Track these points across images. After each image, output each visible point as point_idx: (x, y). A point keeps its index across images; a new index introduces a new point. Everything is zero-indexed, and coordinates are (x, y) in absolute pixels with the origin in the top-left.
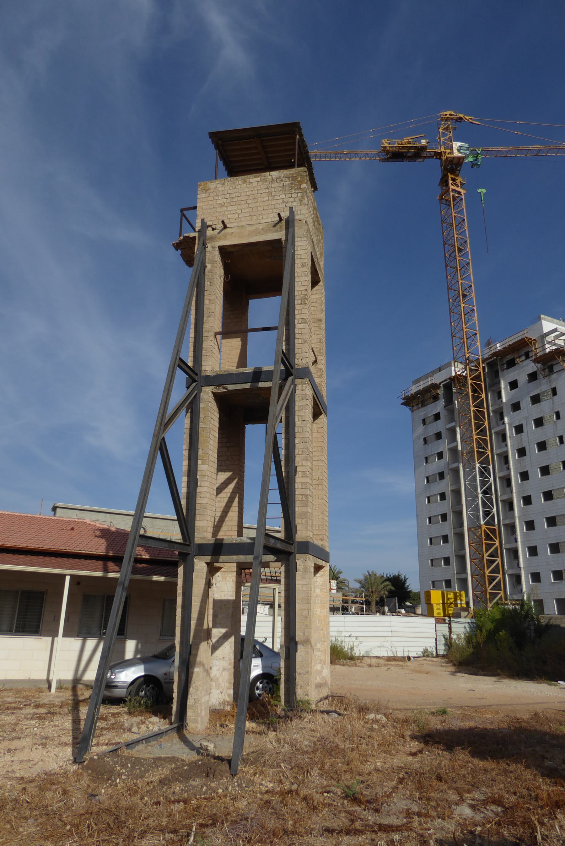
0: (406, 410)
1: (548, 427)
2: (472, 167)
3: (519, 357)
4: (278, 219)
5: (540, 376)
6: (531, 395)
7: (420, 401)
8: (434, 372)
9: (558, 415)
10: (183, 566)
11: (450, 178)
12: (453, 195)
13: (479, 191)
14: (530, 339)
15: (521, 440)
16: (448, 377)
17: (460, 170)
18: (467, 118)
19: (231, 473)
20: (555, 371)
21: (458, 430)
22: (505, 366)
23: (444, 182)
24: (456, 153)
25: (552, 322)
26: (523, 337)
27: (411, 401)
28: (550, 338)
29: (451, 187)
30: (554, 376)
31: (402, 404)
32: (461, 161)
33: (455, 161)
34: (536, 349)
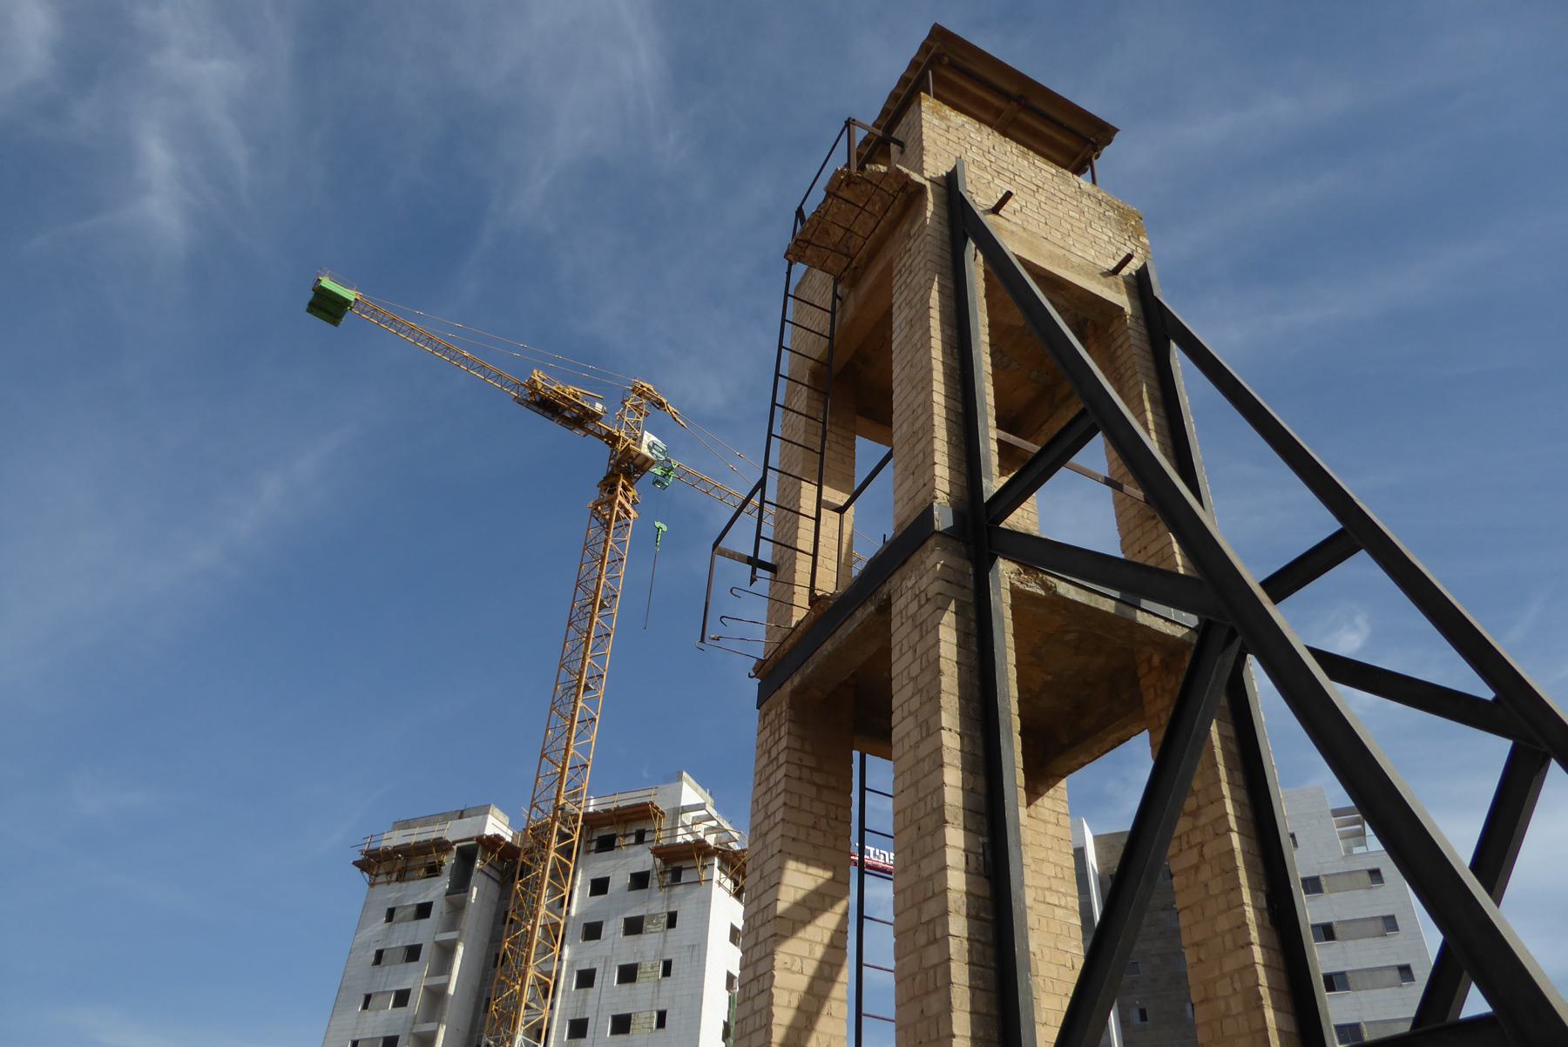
0: (361, 879)
1: (643, 985)
3: (625, 836)
4: (1113, 264)
5: (654, 883)
6: (628, 915)
7: (399, 866)
8: (446, 817)
9: (667, 968)
13: (658, 524)
15: (584, 1001)
16: (475, 834)
19: (828, 875)
21: (460, 950)
22: (594, 846)
23: (609, 485)
24: (645, 450)
26: (647, 800)
27: (376, 863)
28: (687, 818)
29: (620, 498)
30: (679, 890)
31: (356, 863)
33: (638, 461)
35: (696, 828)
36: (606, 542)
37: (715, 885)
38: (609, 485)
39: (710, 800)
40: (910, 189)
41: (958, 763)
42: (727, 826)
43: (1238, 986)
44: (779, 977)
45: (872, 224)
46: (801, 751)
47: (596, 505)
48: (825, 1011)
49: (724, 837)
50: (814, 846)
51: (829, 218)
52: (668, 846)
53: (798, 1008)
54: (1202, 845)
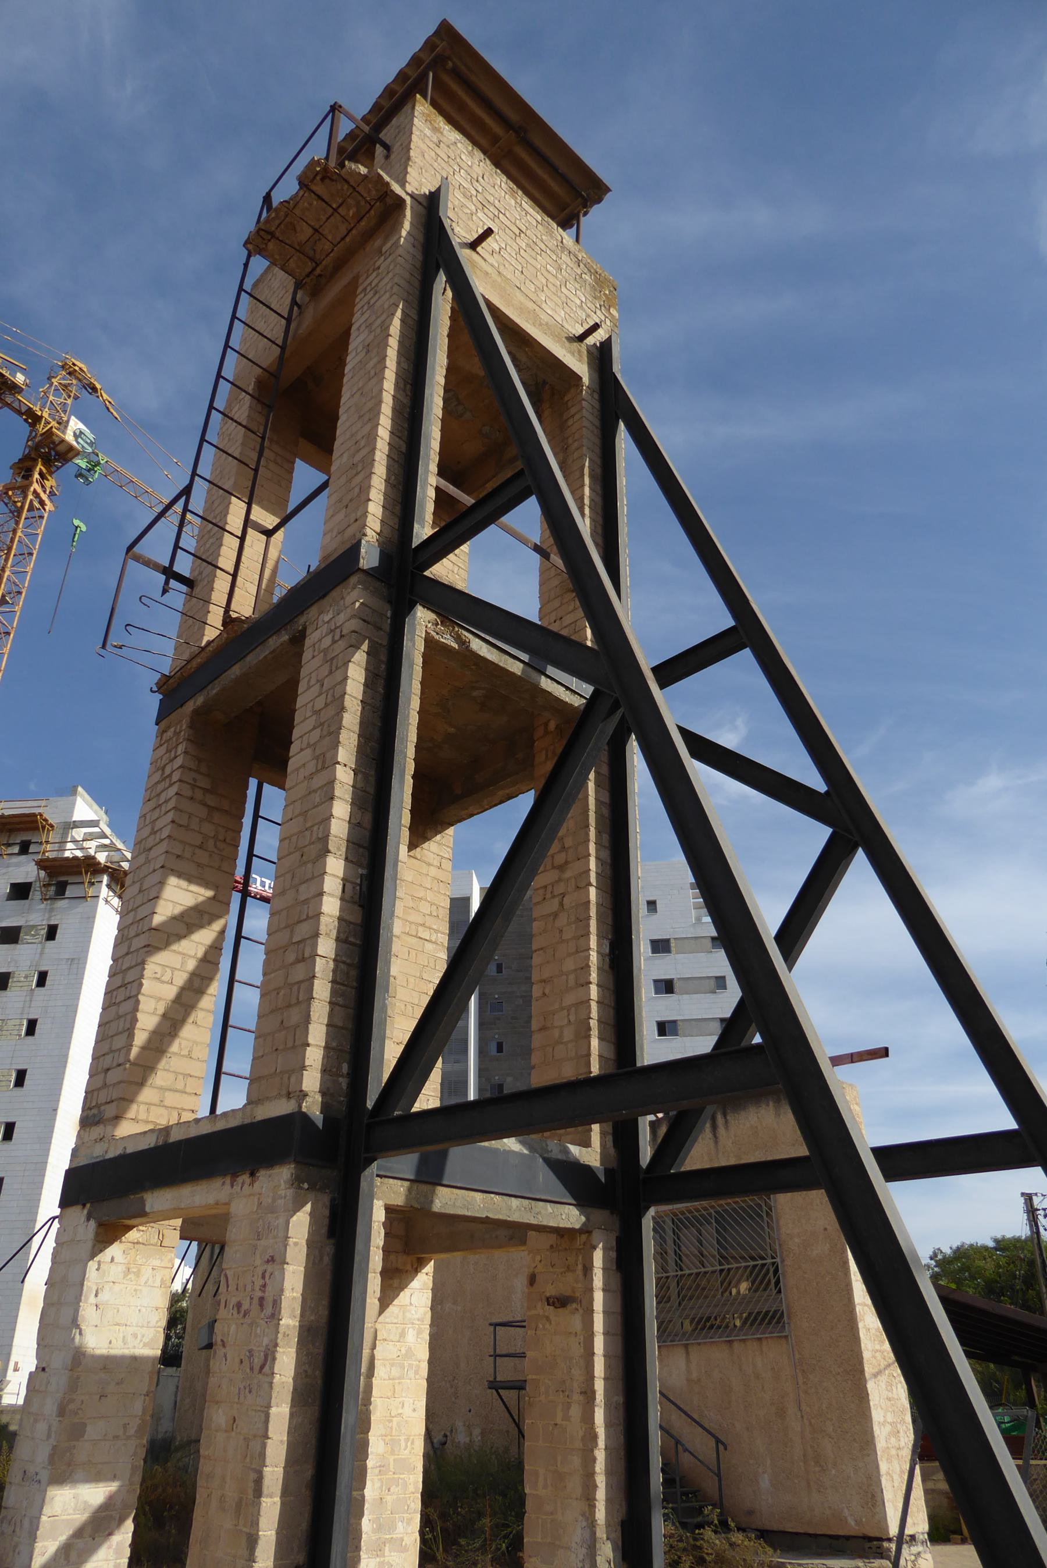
2: (76, 476)
3: (9, 845)
4: (580, 331)
5: (35, 894)
9: (42, 979)
10: (308, 1207)
11: (38, 469)
12: (31, 501)
13: (76, 522)
14: (46, 820)
17: (58, 468)
18: (105, 396)
19: (210, 893)
20: (68, 894)
24: (69, 437)
25: (91, 807)
26: (36, 811)
28: (78, 833)
30: (61, 904)
32: (70, 455)
33: (61, 448)
34: (47, 842)
35: (86, 844)
36: (15, 531)
37: (101, 902)
38: (24, 468)
39: (105, 817)
40: (389, 201)
41: (348, 797)
42: (120, 845)
43: (572, 1018)
44: (147, 984)
45: (343, 229)
46: (197, 771)
47: (7, 489)
48: (191, 1020)
49: (116, 857)
50: (199, 865)
51: (297, 212)
52: (54, 860)
53: (164, 1016)
54: (563, 895)
